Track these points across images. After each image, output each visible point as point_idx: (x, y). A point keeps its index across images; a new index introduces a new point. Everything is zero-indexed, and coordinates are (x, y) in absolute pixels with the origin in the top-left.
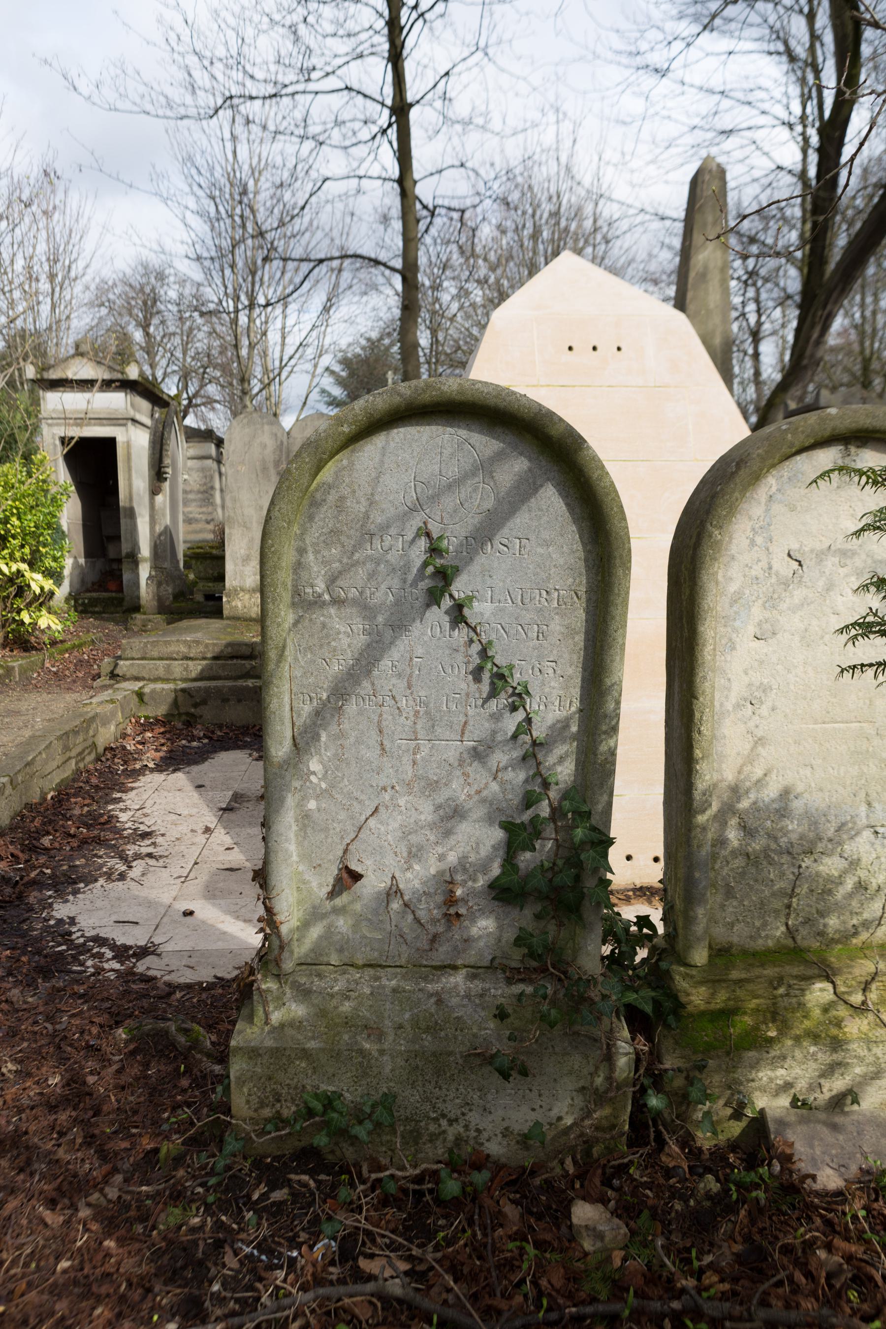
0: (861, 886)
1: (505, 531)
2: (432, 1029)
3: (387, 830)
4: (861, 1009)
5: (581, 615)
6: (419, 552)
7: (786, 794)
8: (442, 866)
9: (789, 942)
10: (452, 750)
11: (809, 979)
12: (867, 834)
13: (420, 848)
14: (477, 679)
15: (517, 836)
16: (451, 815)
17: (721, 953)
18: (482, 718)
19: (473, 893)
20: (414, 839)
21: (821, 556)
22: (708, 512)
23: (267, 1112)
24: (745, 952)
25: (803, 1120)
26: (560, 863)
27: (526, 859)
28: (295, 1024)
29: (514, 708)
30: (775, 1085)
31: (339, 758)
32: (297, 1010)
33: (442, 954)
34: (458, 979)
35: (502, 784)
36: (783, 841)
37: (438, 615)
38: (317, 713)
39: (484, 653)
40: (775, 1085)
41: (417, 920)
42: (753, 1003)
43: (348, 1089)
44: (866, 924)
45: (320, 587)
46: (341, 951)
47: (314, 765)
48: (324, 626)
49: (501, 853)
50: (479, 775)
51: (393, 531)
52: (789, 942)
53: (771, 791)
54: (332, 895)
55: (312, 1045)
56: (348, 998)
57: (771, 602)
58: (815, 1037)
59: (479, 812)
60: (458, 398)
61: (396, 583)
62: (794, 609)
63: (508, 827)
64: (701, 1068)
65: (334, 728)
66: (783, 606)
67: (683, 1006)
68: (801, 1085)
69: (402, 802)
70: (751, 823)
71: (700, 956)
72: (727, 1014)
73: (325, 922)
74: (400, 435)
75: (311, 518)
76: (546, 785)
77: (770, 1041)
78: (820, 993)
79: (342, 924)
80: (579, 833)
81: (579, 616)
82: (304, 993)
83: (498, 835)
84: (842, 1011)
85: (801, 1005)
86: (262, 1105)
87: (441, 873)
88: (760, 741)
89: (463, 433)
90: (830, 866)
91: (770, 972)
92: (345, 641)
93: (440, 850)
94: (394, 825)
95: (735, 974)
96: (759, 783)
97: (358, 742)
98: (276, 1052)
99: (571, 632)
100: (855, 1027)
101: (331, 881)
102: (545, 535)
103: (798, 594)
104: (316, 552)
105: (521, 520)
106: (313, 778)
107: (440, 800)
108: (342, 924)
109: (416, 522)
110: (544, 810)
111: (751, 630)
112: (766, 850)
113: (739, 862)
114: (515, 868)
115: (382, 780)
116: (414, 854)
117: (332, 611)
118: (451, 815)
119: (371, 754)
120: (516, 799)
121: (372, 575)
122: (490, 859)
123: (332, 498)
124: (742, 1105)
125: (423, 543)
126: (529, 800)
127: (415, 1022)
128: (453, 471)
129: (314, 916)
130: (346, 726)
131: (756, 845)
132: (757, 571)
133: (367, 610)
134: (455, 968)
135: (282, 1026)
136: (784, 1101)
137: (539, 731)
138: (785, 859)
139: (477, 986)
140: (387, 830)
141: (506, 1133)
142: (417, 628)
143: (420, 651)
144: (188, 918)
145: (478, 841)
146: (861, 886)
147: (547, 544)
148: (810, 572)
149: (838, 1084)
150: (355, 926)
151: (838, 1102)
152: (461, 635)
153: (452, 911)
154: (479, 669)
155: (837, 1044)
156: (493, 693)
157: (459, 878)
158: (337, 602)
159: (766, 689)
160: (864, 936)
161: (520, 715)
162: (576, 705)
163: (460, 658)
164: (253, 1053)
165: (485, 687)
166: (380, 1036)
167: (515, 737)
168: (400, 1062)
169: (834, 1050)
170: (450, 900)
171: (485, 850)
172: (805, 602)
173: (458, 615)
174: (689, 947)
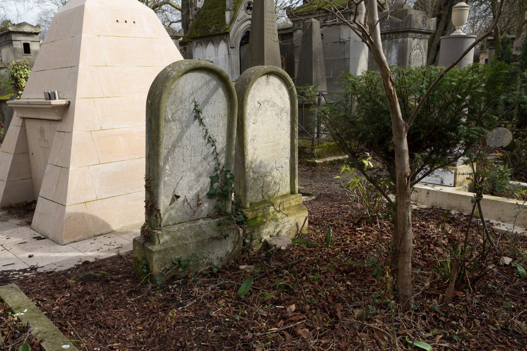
0: (275, 183)
1: (211, 100)
2: (199, 235)
3: (184, 183)
4: (279, 212)
5: (226, 120)
6: (193, 107)
7: (261, 162)
8: (196, 191)
9: (263, 199)
10: (199, 158)
11: (269, 206)
12: (275, 170)
13: (192, 187)
14: (205, 139)
15: (213, 179)
16: (200, 175)
17: (251, 204)
18: (208, 149)
19: (203, 197)
20: (190, 184)
21: (264, 102)
22: (244, 93)
23: (163, 269)
24: (255, 203)
25: (274, 239)
26: (223, 185)
27: (216, 185)
28: (166, 242)
29: (213, 145)
30: (267, 233)
31: (173, 164)
32: (166, 237)
33: (196, 217)
34: (201, 221)
35: (210, 166)
36: (261, 174)
37: (197, 122)
38: (168, 152)
39: (207, 132)
40: (267, 233)
41: (191, 207)
42: (260, 215)
43: (182, 255)
44: (276, 192)
45: (170, 117)
46: (172, 220)
47: (167, 167)
48: (170, 127)
49: (210, 185)
50: (205, 163)
51: (187, 101)
52: (263, 199)
53: (258, 162)
54: (170, 204)
55: (174, 245)
56: (179, 231)
57: (256, 114)
58: (272, 219)
59: (205, 174)
60: (205, 66)
61: (188, 115)
62: (260, 116)
63: (211, 178)
64: (253, 232)
65: (172, 156)
66: (258, 115)
67: (247, 218)
68: (271, 232)
69: (188, 174)
70: (255, 170)
71: (248, 205)
72: (256, 218)
73: (168, 213)
74: (189, 75)
75: (168, 98)
76: (219, 164)
77: (265, 222)
78: (272, 209)
79: (173, 212)
80: (228, 176)
81: (225, 121)
82: (168, 232)
83: (209, 180)
84: (276, 213)
85: (269, 213)
86: (161, 267)
87: (196, 193)
88: (255, 149)
89: (203, 74)
90: (269, 179)
91: (262, 206)
92: (175, 131)
93: (196, 186)
94: (186, 181)
95: (256, 208)
96: (256, 160)
97: (178, 159)
98: (165, 250)
99: (224, 125)
100: (279, 215)
101: (170, 200)
102: (219, 100)
103: (261, 112)
104: (169, 107)
105: (215, 97)
106: (167, 171)
107: (196, 173)
108: (173, 212)
109: (192, 98)
110: (219, 172)
111: (252, 122)
112: (258, 177)
113: (252, 181)
114: (213, 188)
115: (184, 169)
116: (191, 188)
117: (172, 123)
118: (200, 175)
119: (181, 162)
120: (213, 169)
121: (182, 113)
122: (207, 187)
123: (173, 92)
124: (261, 239)
125: (193, 104)
126: (216, 170)
127: (195, 235)
128: (200, 85)
129: (167, 211)
130: (175, 155)
131: (255, 176)
132: (252, 107)
133: (181, 122)
134: (199, 219)
135: (163, 243)
136: (268, 236)
137: (218, 151)
138: (261, 178)
139: (207, 221)
140: (184, 183)
141: (218, 258)
142: (192, 127)
143: (192, 133)
144: (32, 258)
145: (206, 181)
146: (275, 183)
147: (219, 102)
148: (262, 106)
149: (278, 230)
150: (176, 213)
151: (278, 234)
152: (201, 128)
153: (199, 203)
154: (206, 136)
155: (277, 220)
156: (209, 141)
157: (200, 194)
158: (174, 120)
159: (255, 136)
160: (276, 195)
161: (214, 147)
162: (225, 143)
163: (201, 134)
164: (159, 252)
165: (207, 141)
166: (188, 240)
167: (213, 153)
168: (194, 245)
169: (276, 222)
170: (199, 200)
171: (206, 185)
172: (262, 114)
173: (201, 122)
174: (246, 204)
